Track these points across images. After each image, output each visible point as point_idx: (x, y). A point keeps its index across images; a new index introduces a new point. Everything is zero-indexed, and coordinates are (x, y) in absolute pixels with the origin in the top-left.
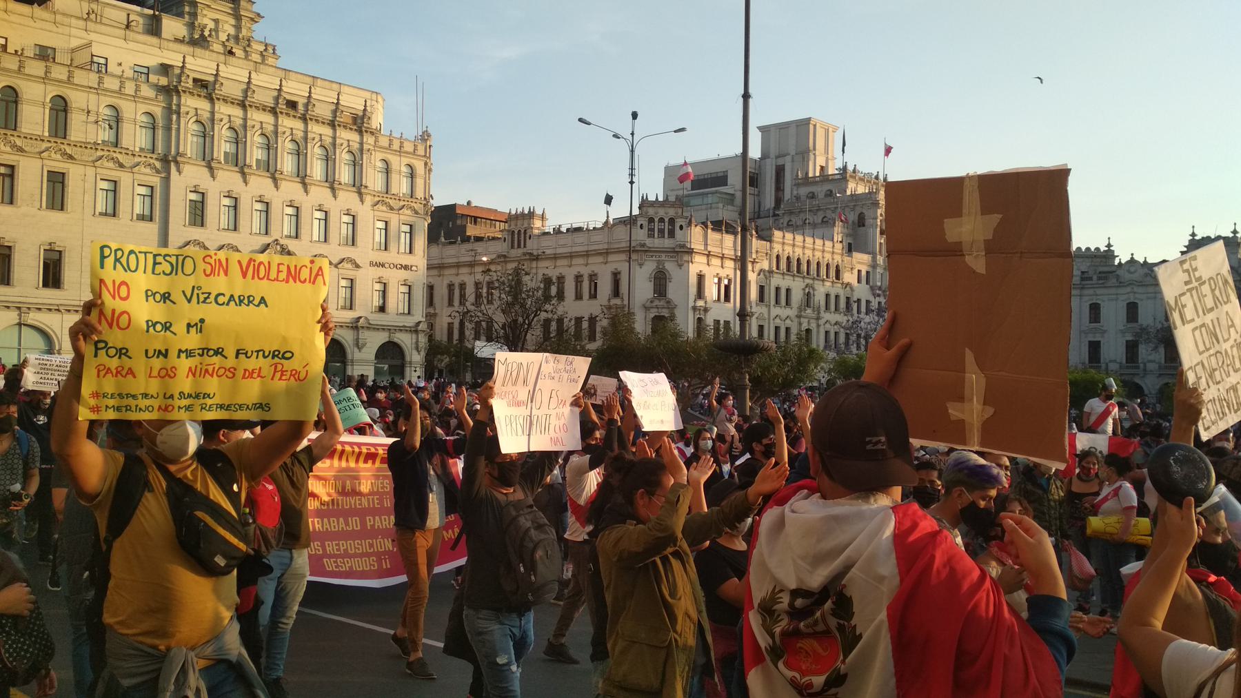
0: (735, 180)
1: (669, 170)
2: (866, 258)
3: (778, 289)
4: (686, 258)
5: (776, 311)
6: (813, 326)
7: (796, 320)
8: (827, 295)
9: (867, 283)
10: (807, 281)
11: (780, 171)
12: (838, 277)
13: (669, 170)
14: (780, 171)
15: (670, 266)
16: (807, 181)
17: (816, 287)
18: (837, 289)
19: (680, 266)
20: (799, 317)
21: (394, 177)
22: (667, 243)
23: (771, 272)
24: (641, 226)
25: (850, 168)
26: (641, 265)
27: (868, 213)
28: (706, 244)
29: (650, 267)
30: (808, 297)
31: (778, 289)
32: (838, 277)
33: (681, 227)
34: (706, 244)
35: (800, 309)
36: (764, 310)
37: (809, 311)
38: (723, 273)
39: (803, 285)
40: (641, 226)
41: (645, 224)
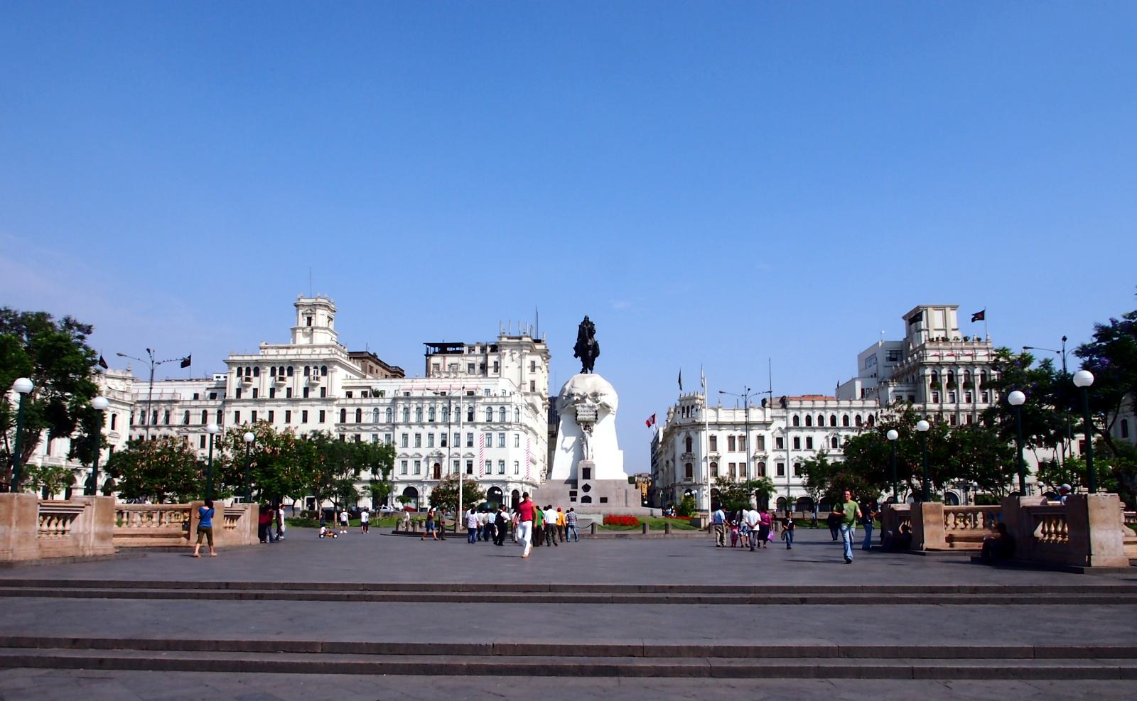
0: (882, 359)
3: (797, 440)
4: (700, 428)
15: (692, 434)
17: (840, 433)
19: (697, 433)
21: (494, 414)
22: (690, 421)
23: (788, 429)
24: (679, 413)
26: (679, 435)
29: (683, 435)
31: (797, 440)
33: (697, 410)
36: (784, 455)
38: (737, 434)
40: (679, 413)
41: (681, 411)
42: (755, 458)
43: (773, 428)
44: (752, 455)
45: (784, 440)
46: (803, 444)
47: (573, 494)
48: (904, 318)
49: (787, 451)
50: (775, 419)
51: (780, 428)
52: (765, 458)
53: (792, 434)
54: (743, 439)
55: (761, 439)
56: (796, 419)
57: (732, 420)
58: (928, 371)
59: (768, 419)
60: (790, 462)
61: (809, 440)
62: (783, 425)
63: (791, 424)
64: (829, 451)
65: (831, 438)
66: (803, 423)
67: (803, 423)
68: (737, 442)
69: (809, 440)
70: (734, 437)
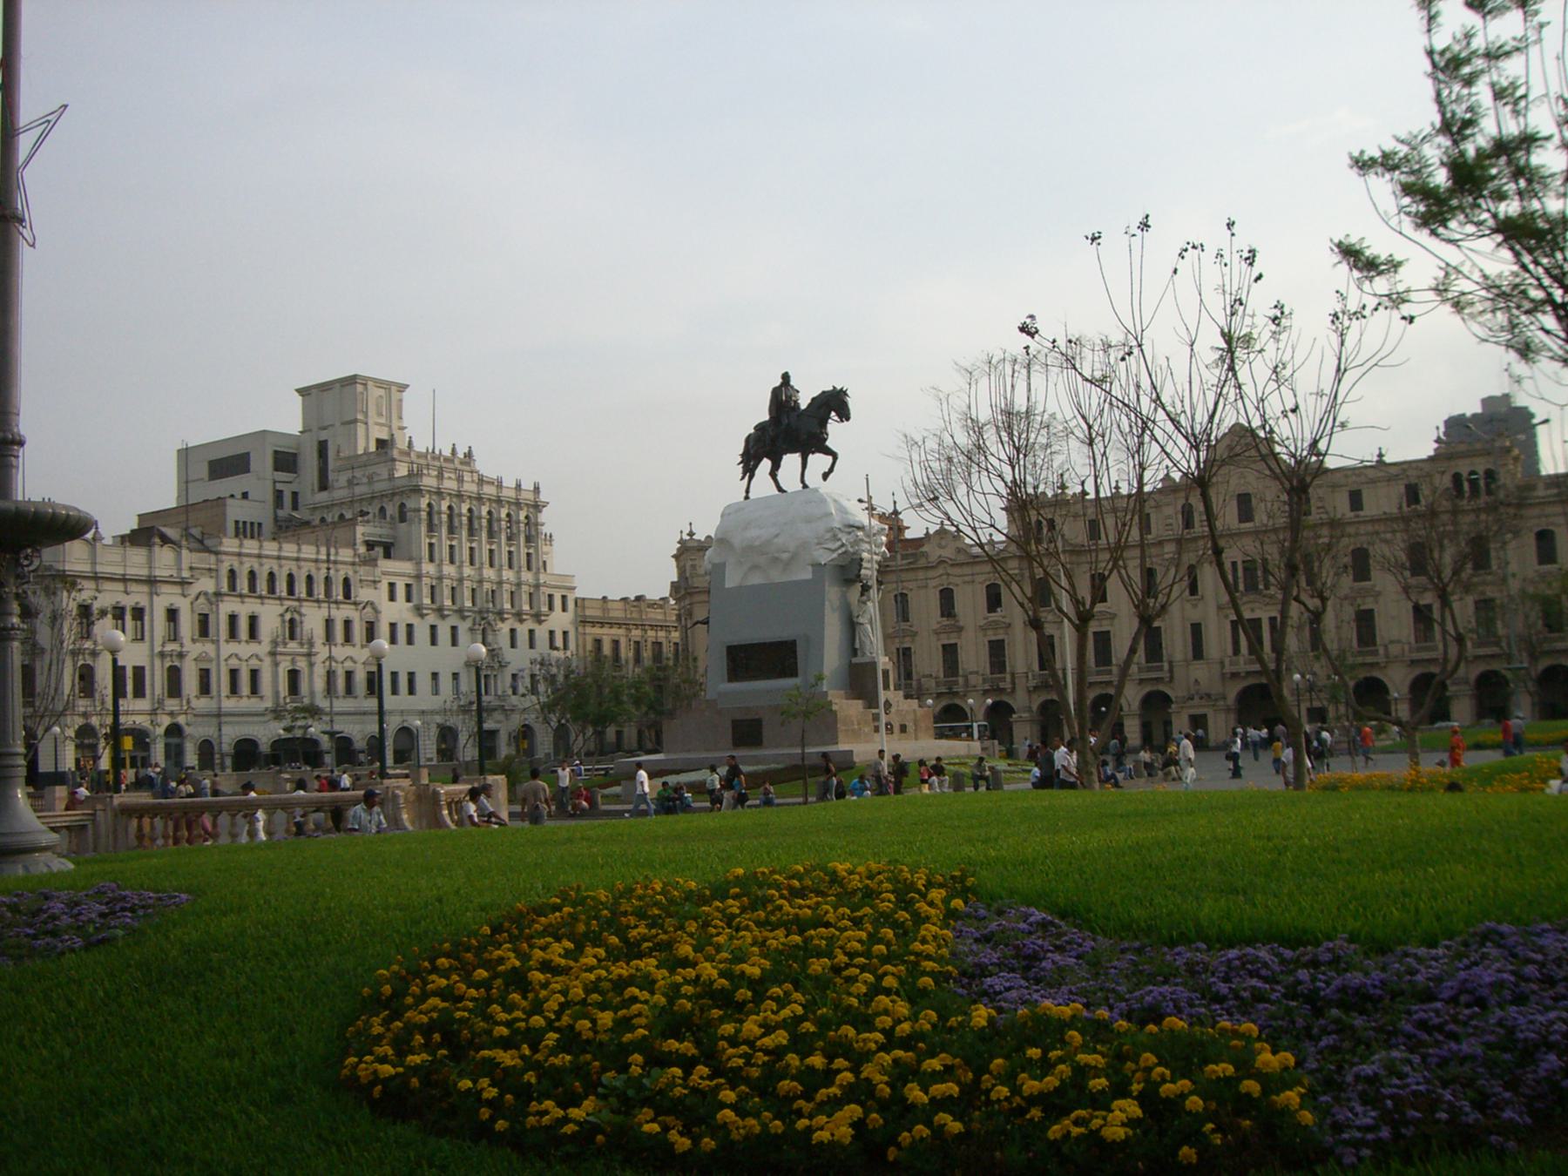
1: (185, 455)
2: (407, 567)
3: (233, 619)
5: (228, 648)
6: (302, 664)
7: (268, 661)
8: (329, 623)
9: (408, 600)
10: (288, 603)
11: (323, 448)
12: (347, 595)
13: (185, 455)
14: (323, 448)
16: (354, 463)
17: (303, 610)
18: (340, 614)
20: (273, 654)
23: (218, 594)
25: (401, 444)
27: (410, 504)
28: (94, 563)
30: (293, 628)
31: (233, 619)
32: (347, 595)
34: (94, 563)
35: (275, 643)
36: (209, 648)
37: (293, 646)
38: (128, 602)
39: (281, 610)
42: (162, 655)
43: (194, 590)
44: (158, 649)
45: (212, 619)
46: (243, 625)
47: (876, 718)
48: (304, 392)
49: (216, 642)
50: (196, 573)
51: (206, 594)
52: (181, 655)
53: (228, 606)
54: (138, 613)
55: (172, 614)
56: (232, 574)
57: (120, 571)
58: (424, 502)
59: (186, 574)
60: (223, 663)
61: (253, 620)
62: (211, 589)
63: (225, 589)
64: (285, 644)
65: (288, 616)
66: (243, 584)
67: (243, 584)
68: (128, 617)
69: (253, 620)
70: (123, 609)
